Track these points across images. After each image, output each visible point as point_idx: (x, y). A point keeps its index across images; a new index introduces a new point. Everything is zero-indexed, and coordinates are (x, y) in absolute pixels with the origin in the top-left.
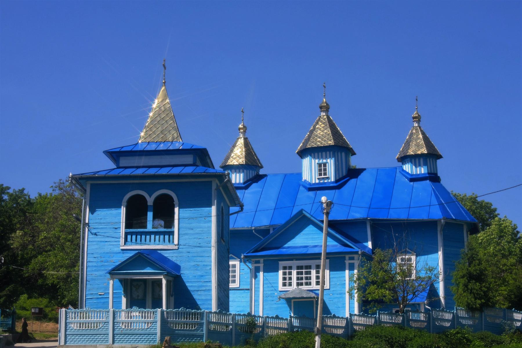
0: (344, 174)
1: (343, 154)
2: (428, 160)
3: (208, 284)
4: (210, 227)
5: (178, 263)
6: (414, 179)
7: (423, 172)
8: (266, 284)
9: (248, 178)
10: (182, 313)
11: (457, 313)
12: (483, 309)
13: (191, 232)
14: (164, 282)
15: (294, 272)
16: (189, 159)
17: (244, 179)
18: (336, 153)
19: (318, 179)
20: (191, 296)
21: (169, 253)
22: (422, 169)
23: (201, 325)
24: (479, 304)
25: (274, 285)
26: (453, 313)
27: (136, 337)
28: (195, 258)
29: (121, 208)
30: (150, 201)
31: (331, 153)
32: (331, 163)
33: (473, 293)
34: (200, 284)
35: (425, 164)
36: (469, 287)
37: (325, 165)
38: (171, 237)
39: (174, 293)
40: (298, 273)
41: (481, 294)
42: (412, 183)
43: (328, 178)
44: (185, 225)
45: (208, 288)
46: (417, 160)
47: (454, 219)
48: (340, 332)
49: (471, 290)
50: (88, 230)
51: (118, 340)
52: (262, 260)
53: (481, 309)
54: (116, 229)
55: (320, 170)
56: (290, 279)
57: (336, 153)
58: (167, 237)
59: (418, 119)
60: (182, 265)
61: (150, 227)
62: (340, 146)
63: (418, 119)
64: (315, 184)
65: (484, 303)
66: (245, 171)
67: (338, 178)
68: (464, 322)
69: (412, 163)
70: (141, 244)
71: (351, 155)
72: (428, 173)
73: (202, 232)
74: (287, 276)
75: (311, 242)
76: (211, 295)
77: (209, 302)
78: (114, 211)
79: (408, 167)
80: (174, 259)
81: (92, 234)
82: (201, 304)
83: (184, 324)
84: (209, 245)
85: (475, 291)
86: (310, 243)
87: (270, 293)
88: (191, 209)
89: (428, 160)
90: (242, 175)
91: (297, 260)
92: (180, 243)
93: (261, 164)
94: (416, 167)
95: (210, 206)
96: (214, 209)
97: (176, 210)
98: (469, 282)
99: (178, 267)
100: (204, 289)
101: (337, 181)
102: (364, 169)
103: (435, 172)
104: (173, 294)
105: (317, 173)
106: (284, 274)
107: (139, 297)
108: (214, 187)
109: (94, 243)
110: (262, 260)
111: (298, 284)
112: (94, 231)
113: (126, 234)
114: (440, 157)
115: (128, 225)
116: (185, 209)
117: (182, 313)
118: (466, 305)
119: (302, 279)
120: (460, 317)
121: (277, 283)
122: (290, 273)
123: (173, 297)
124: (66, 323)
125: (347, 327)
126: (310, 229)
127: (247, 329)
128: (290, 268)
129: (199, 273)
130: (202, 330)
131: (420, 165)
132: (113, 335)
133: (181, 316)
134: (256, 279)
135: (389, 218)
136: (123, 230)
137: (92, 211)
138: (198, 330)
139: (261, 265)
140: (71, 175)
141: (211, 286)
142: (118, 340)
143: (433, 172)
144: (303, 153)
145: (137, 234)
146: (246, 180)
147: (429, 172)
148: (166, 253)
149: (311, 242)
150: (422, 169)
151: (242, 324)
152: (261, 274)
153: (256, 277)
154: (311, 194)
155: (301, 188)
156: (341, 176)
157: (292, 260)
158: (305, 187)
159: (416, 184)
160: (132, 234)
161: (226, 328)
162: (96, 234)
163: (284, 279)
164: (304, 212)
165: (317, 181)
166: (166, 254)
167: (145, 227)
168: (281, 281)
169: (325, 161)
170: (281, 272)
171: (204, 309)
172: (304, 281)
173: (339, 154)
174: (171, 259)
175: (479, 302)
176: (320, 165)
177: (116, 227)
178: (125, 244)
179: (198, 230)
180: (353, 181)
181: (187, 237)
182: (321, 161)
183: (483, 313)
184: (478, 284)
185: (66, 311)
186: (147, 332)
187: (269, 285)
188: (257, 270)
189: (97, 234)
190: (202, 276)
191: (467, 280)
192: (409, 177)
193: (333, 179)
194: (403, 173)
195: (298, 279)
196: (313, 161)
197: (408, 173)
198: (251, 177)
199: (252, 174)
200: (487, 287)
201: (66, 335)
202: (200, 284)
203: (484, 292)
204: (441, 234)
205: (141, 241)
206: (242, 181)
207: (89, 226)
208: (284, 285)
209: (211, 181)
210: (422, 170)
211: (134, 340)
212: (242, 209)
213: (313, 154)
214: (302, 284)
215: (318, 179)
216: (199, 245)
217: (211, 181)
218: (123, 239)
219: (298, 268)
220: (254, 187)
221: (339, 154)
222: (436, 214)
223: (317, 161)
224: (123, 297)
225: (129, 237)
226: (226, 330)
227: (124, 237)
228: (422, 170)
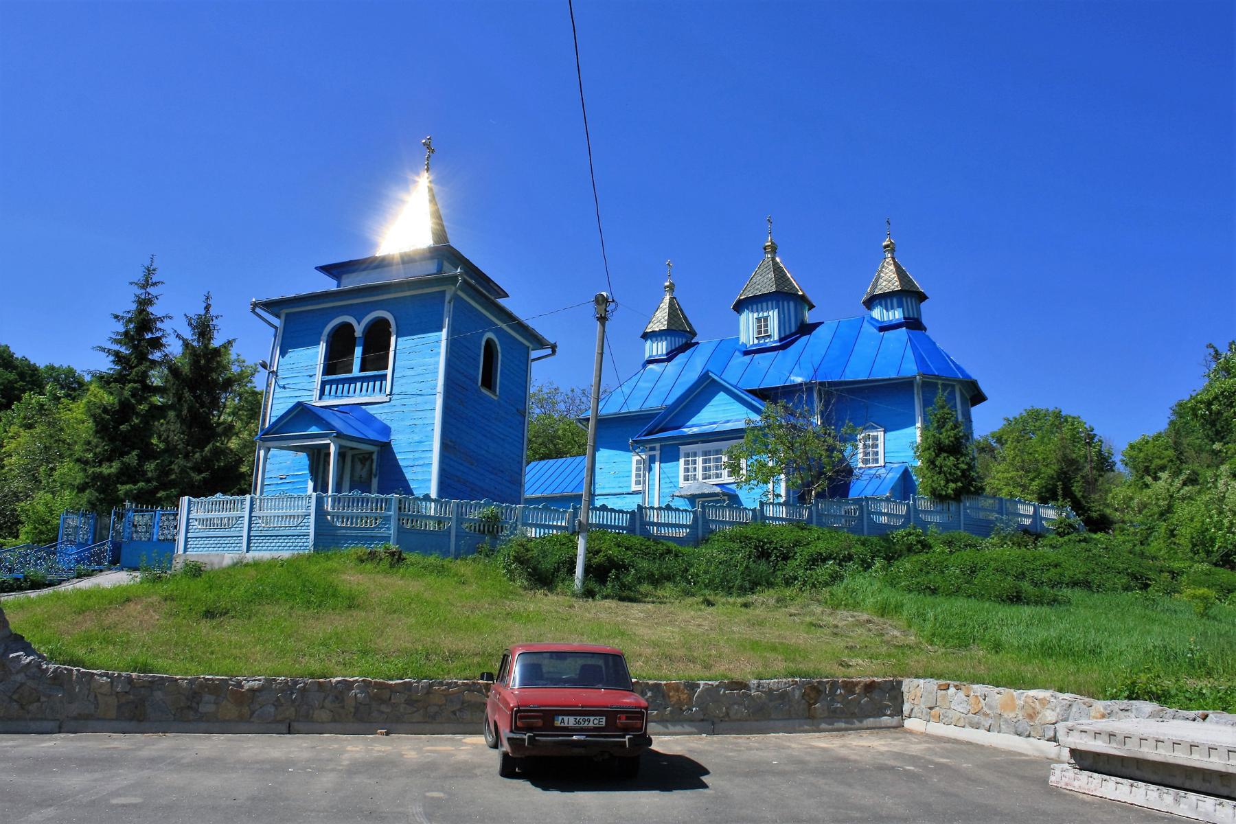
0: (793, 330)
1: (792, 304)
2: (904, 300)
3: (428, 455)
4: (437, 363)
5: (388, 423)
6: (884, 328)
7: (897, 317)
8: (664, 478)
9: (673, 348)
10: (353, 499)
11: (915, 504)
12: (962, 498)
13: (411, 372)
14: (333, 449)
15: (700, 460)
17: (667, 349)
18: (781, 303)
19: (757, 338)
20: (403, 474)
21: (376, 409)
22: (896, 313)
23: (387, 518)
24: (953, 490)
25: (673, 480)
26: (908, 504)
27: (281, 541)
28: (412, 414)
29: (319, 344)
30: (359, 331)
31: (774, 302)
32: (773, 316)
33: (945, 473)
34: (417, 455)
35: (900, 305)
36: (937, 463)
37: (766, 319)
38: (384, 382)
40: (705, 461)
41: (955, 474)
42: (882, 333)
43: (769, 336)
44: (403, 363)
45: (427, 462)
46: (889, 301)
47: (935, 375)
48: (682, 533)
49: (941, 467)
50: (276, 382)
51: (256, 545)
52: (658, 446)
53: (958, 496)
54: (311, 376)
55: (760, 327)
57: (781, 303)
59: (891, 248)
60: (393, 426)
61: (356, 371)
62: (785, 293)
63: (891, 248)
64: (754, 345)
65: (961, 488)
66: (669, 338)
67: (783, 336)
68: (928, 518)
69: (881, 306)
70: (336, 396)
71: (807, 308)
72: (905, 318)
73: (425, 372)
75: (722, 416)
76: (430, 472)
77: (427, 484)
78: (309, 351)
79: (877, 313)
80: (382, 418)
81: (280, 387)
82: (415, 488)
83: (357, 518)
84: (434, 391)
85: (946, 469)
86: (721, 417)
87: (667, 491)
88: (415, 337)
89: (904, 300)
90: (664, 343)
91: (703, 442)
92: (393, 392)
93: (690, 325)
94: (887, 310)
95: (440, 329)
96: (444, 333)
97: (393, 339)
98: (937, 455)
99: (386, 430)
100: (421, 462)
101: (781, 340)
102: (823, 323)
103: (916, 316)
105: (756, 330)
106: (687, 463)
109: (281, 401)
110: (658, 446)
112: (282, 383)
113: (324, 384)
115: (326, 372)
116: (405, 338)
117: (353, 499)
118: (931, 492)
120: (921, 510)
121: (678, 477)
122: (695, 462)
123: (377, 478)
124: (188, 519)
125: (693, 526)
126: (722, 396)
127: (482, 528)
128: (695, 455)
129: (417, 438)
130: (388, 529)
131: (892, 308)
132: (249, 537)
133: (353, 505)
134: (651, 473)
135: (842, 379)
136: (319, 378)
137: (283, 353)
138: (382, 528)
139: (657, 453)
140: (254, 300)
141: (431, 458)
142: (256, 545)
143: (911, 316)
144: (740, 306)
145: (337, 382)
146: (670, 350)
147: (906, 316)
148: (372, 409)
149: (722, 416)
150: (896, 313)
151: (473, 520)
152: (657, 464)
153: (650, 469)
154: (748, 358)
155: (737, 353)
156: (788, 333)
157: (697, 443)
158: (739, 351)
159: (887, 334)
160: (331, 382)
161: (439, 525)
162: (284, 388)
163: (687, 470)
164: (711, 374)
165: (756, 342)
166: (371, 410)
167: (351, 371)
168: (682, 474)
169: (765, 314)
170: (682, 461)
171: (419, 493)
173: (786, 304)
174: (378, 418)
175: (952, 485)
176: (759, 320)
177: (311, 374)
178: (320, 399)
179: (419, 370)
180: (805, 338)
181: (404, 381)
182: (761, 315)
183: (962, 504)
184: (951, 458)
185: (189, 500)
186: (296, 533)
187: (668, 480)
188: (652, 460)
189: (286, 386)
190: (420, 442)
191: (933, 453)
192: (878, 325)
193: (776, 337)
194: (874, 322)
195: (705, 469)
196: (751, 315)
197: (877, 321)
198: (677, 346)
199: (680, 341)
200: (967, 464)
201: (186, 538)
202: (417, 455)
203: (963, 471)
204: (919, 398)
205: (336, 393)
206: (664, 352)
207: (277, 376)
208: (687, 479)
209: (445, 291)
210: (897, 315)
211: (278, 545)
212: (554, 352)
213: (750, 308)
215: (757, 338)
216: (420, 393)
217: (445, 291)
218: (318, 392)
219: (705, 453)
220: (681, 358)
221: (786, 304)
222: (910, 368)
223: (756, 315)
224: (310, 481)
225: (327, 387)
226: (440, 529)
227: (319, 388)
228: (897, 315)
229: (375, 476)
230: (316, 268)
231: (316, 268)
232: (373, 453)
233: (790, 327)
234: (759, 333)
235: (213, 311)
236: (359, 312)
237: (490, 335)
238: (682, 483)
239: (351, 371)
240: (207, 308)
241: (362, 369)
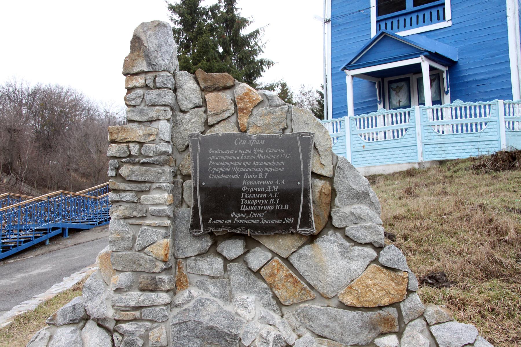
39: (449, 89)
58: (434, 12)
104: (448, 90)
107: (400, 103)
113: (377, 22)
123: (449, 94)
167: (405, 8)
229: (447, 93)
232: (443, 72)
239: (405, 8)
241: (415, 5)
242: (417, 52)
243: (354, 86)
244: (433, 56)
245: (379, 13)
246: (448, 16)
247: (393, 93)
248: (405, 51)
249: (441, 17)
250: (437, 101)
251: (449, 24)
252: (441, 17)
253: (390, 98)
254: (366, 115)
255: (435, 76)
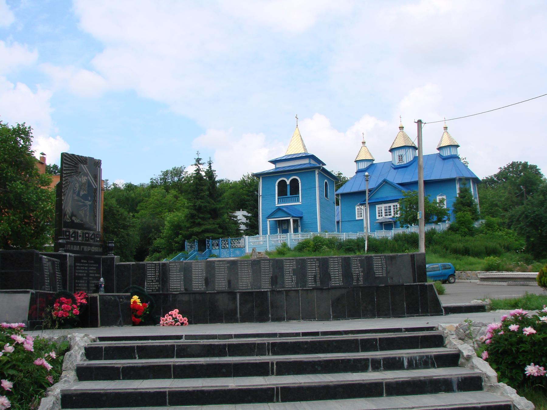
16: (306, 161)
30: (288, 182)
55: (399, 159)
56: (382, 213)
74: (395, 210)
108: (317, 172)
111: (386, 215)
114: (457, 146)
119: (387, 213)
165: (398, 164)
172: (388, 214)
208: (379, 216)
214: (387, 215)
225: (280, 200)
230: (268, 161)
231: (268, 161)
233: (411, 159)
234: (400, 161)
235: (213, 169)
236: (288, 177)
237: (326, 181)
238: (377, 218)
240: (210, 167)
242: (289, 215)
243: (269, 223)
244: (293, 217)
245: (278, 196)
246: (300, 201)
247: (283, 225)
248: (286, 215)
249: (298, 201)
250: (296, 230)
251: (301, 203)
252: (298, 201)
253: (282, 226)
254: (273, 235)
255: (294, 221)
